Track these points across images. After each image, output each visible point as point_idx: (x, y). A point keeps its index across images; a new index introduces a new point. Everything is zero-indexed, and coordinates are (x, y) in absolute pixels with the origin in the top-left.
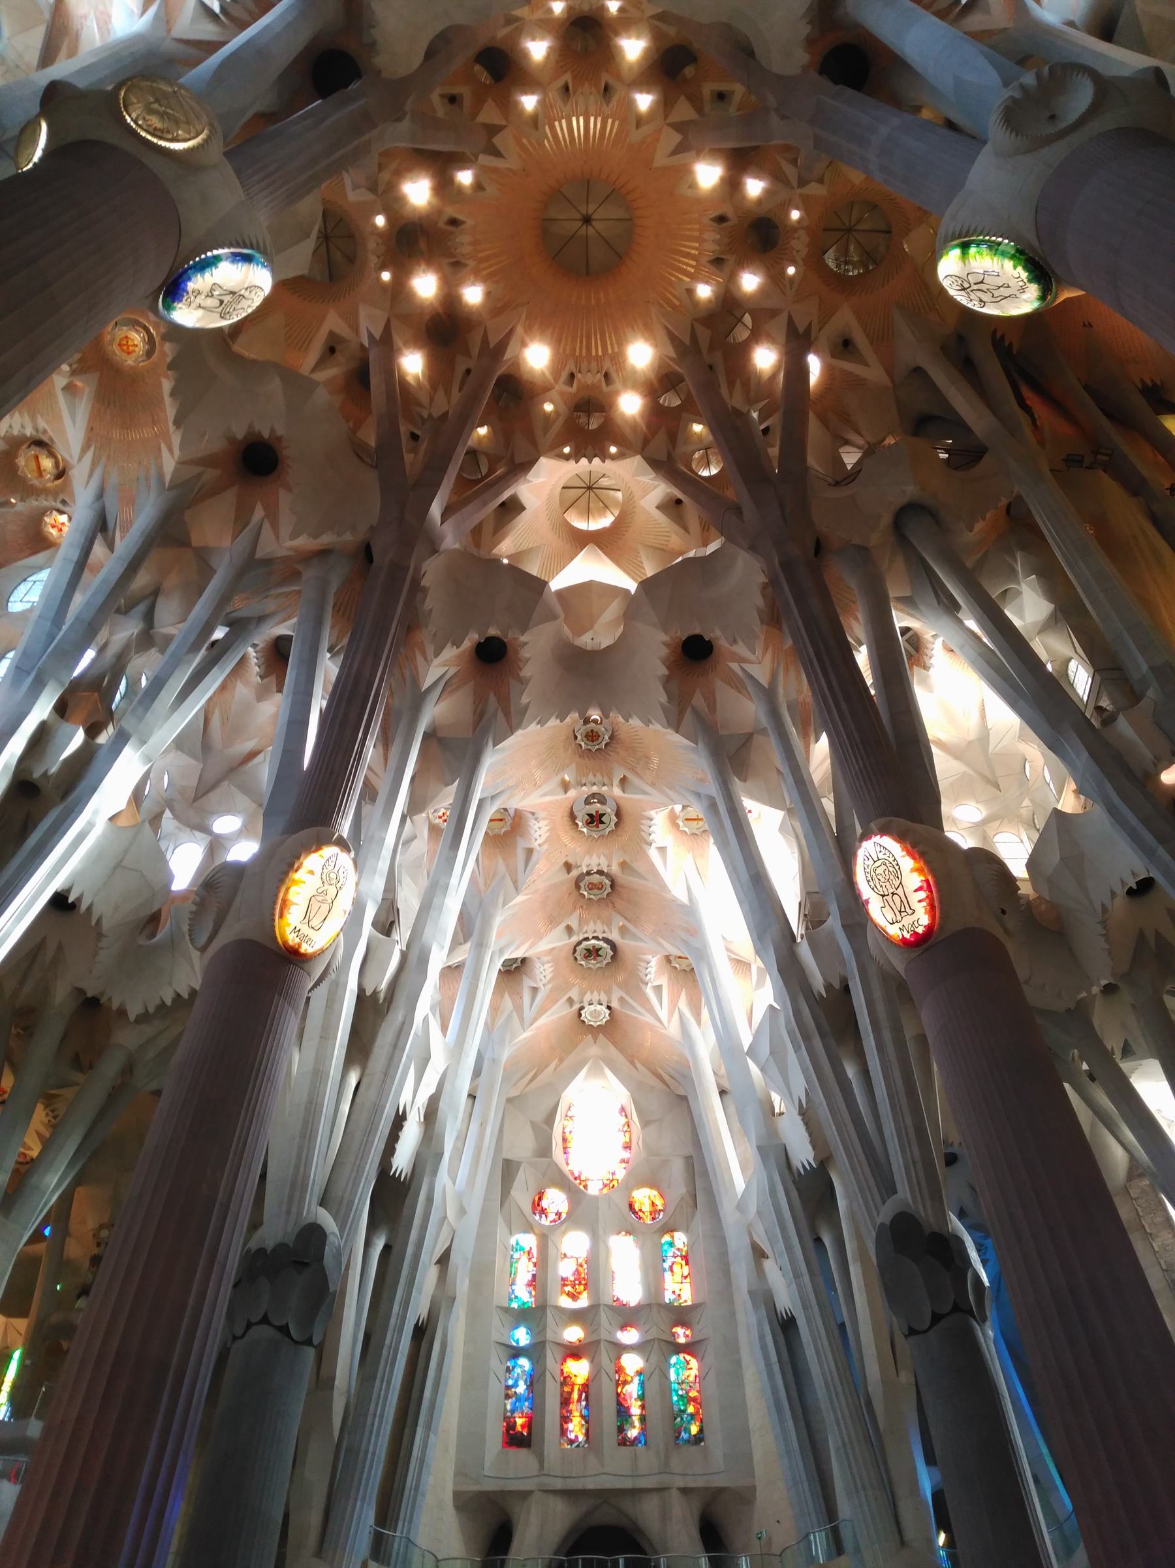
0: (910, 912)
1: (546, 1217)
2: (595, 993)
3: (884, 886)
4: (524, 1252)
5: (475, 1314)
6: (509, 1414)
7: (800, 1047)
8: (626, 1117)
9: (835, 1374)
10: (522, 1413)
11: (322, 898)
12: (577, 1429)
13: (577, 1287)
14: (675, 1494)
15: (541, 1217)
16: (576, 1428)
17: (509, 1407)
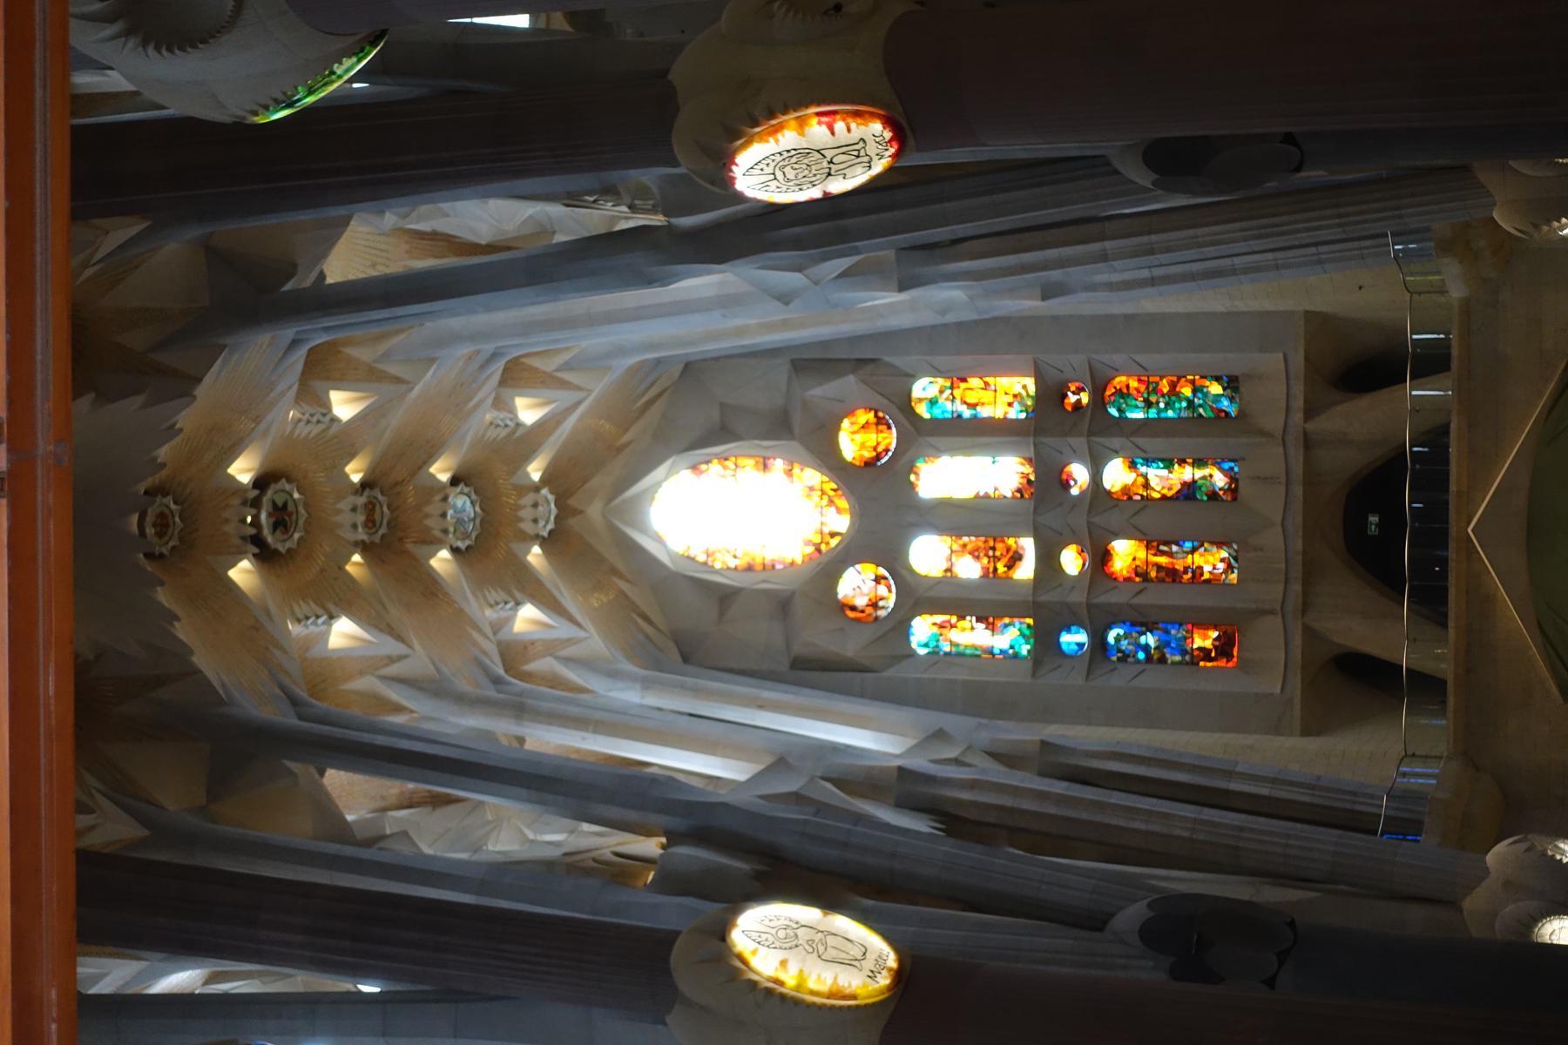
0: (861, 144)
1: (882, 599)
2: (522, 513)
3: (814, 172)
4: (941, 635)
5: (1046, 712)
6: (1187, 658)
7: (856, 247)
8: (708, 462)
9: (1244, 224)
10: (1186, 638)
11: (819, 945)
12: (1211, 559)
13: (998, 553)
14: (1310, 426)
15: (883, 608)
16: (1211, 561)
17: (1178, 658)
